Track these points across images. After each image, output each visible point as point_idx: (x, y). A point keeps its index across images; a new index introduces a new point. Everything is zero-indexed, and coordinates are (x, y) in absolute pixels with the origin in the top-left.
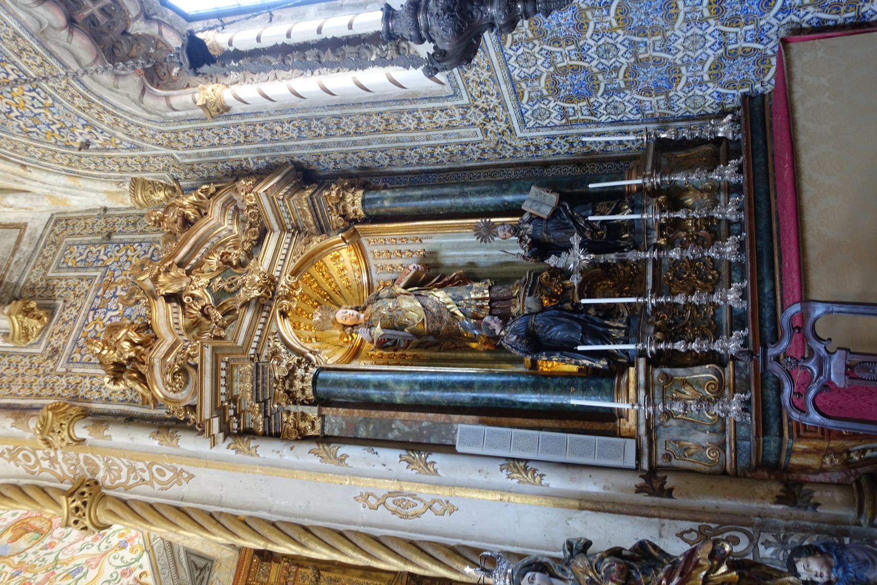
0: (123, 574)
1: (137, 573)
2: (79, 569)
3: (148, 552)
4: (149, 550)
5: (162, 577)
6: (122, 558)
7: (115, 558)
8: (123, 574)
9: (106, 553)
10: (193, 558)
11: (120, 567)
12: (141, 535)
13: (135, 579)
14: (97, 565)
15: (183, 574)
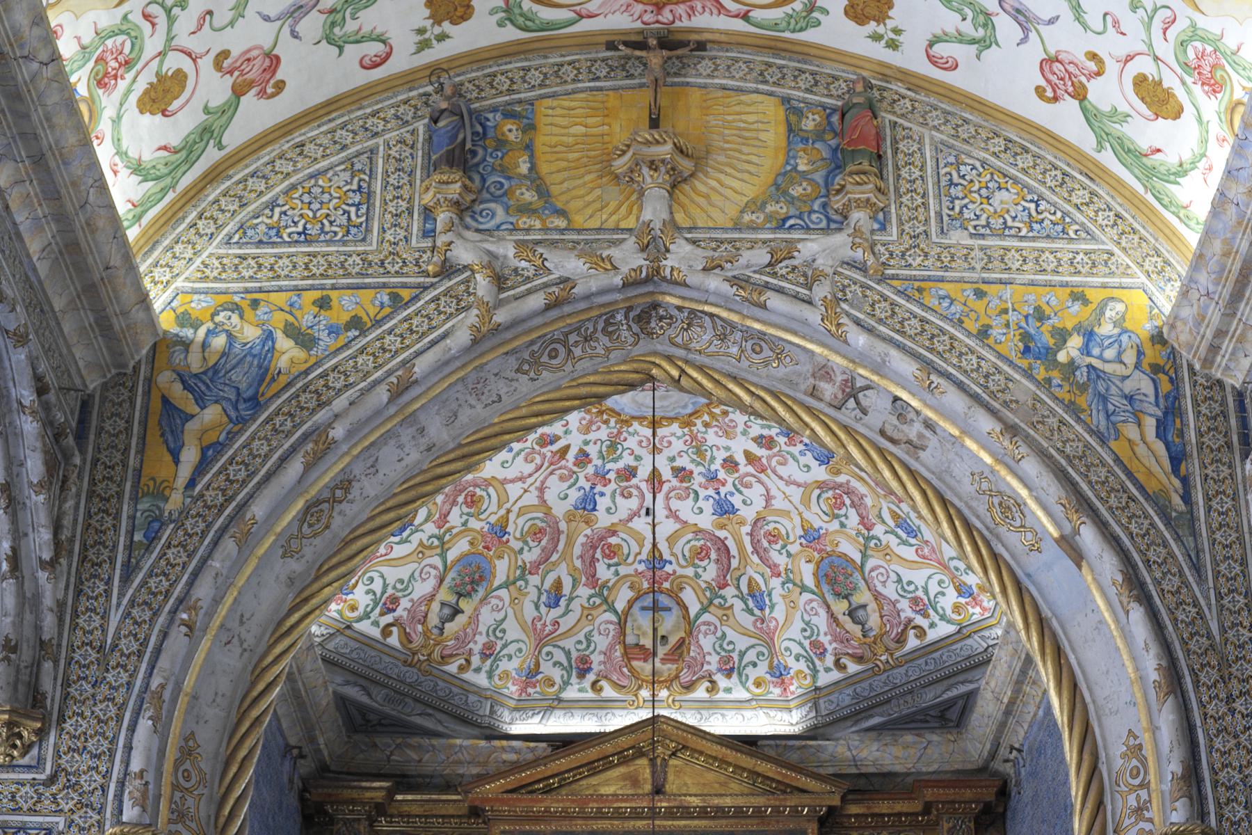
0: (915, 601)
1: (920, 620)
2: (912, 532)
3: (959, 632)
4: (963, 633)
5: (922, 661)
6: (943, 594)
7: (940, 583)
8: (915, 601)
9: (946, 567)
10: (961, 703)
11: (926, 592)
12: (987, 615)
13: (910, 620)
14: (924, 557)
15: (930, 695)
